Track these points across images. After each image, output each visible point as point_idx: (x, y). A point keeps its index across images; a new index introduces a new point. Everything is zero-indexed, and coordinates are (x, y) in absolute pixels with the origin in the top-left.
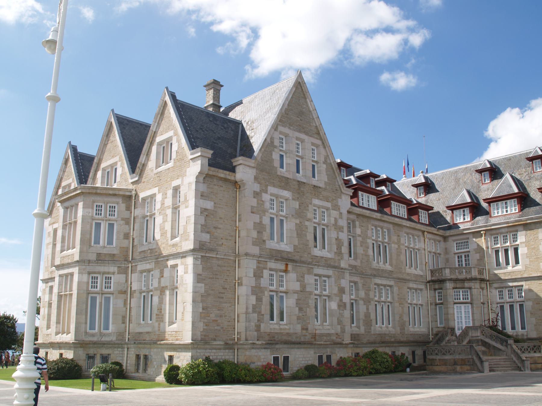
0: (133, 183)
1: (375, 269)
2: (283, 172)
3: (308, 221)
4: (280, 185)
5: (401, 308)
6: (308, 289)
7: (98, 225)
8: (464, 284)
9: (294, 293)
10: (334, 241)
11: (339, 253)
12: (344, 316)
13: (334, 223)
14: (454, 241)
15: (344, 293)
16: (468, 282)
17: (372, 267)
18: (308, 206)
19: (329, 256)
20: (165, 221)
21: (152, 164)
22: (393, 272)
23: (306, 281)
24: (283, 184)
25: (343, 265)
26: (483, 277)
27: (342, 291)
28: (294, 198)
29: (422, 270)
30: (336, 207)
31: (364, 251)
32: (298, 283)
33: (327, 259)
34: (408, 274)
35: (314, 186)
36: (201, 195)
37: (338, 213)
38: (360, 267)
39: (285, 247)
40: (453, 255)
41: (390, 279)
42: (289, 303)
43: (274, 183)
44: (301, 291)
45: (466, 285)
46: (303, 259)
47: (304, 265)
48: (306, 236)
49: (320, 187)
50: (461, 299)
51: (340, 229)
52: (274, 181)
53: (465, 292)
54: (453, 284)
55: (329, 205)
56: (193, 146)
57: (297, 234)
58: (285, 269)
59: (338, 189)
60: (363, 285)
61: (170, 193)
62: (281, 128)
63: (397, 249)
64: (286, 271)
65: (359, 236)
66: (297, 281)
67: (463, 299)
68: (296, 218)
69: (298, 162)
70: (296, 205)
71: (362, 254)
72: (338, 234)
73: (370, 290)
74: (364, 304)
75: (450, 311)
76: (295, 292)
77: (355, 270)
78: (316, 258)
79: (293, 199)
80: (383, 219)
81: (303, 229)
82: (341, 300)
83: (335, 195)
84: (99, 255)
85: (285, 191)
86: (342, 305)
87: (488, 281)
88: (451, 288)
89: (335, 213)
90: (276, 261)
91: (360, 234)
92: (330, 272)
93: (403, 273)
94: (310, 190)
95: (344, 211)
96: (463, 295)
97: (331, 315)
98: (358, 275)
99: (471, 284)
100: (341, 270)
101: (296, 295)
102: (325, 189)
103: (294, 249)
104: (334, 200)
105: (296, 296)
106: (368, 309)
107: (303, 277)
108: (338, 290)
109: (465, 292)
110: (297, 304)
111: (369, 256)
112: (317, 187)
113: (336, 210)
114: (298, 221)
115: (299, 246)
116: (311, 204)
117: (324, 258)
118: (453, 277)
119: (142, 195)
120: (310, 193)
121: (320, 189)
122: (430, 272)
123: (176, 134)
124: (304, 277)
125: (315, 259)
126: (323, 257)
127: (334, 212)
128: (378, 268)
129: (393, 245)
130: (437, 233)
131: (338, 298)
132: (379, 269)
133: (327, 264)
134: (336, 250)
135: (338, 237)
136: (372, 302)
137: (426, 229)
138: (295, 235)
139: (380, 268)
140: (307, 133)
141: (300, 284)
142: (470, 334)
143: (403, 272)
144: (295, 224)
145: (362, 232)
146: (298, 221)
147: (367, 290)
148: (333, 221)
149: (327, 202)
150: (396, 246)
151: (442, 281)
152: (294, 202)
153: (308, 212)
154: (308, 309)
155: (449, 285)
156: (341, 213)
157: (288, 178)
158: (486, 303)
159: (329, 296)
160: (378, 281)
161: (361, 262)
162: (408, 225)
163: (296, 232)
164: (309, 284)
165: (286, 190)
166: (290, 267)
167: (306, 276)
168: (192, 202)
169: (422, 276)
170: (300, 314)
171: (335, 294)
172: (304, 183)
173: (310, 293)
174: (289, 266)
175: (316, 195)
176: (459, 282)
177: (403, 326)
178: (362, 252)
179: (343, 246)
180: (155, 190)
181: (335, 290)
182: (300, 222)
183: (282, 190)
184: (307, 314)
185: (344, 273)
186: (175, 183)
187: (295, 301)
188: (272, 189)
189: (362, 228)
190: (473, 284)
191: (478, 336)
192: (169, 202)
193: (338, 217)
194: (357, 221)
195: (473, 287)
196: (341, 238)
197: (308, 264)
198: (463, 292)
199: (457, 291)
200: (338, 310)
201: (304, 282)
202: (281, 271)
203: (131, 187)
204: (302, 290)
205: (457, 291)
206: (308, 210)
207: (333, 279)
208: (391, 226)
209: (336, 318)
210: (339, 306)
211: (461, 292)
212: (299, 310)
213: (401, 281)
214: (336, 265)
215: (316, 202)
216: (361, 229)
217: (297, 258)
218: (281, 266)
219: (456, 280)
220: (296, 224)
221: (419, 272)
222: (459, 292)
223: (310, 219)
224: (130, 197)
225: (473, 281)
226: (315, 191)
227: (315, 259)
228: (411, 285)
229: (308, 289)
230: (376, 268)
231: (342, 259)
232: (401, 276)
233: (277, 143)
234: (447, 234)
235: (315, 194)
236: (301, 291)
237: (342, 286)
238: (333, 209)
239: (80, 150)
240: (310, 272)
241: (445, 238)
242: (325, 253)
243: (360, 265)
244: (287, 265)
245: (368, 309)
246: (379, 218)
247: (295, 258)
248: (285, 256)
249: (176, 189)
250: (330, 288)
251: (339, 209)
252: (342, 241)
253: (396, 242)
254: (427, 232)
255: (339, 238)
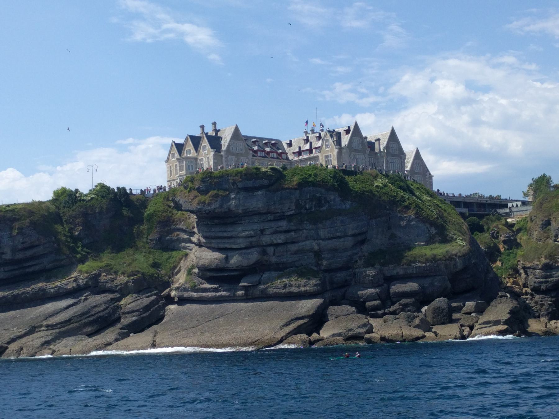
0: (197, 155)
7: (189, 166)
20: (206, 165)
21: (201, 151)
30: (248, 158)
36: (214, 159)
56: (212, 148)
61: (207, 158)
62: (232, 141)
69: (237, 148)
84: (190, 173)
119: (199, 158)
123: (207, 144)
140: (239, 140)
168: (212, 161)
180: (203, 157)
186: (208, 156)
188: (230, 156)
192: (207, 160)
203: (196, 156)
224: (196, 158)
233: (231, 145)
239: (176, 142)
249: (208, 158)
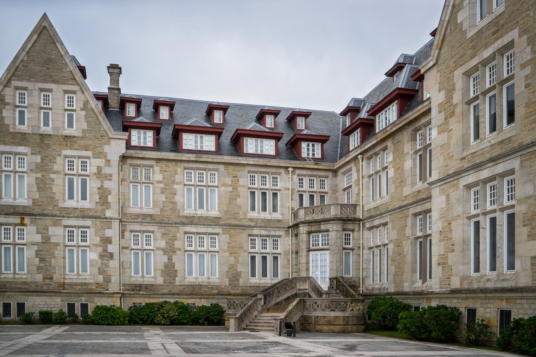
1: (186, 217)
2: (24, 128)
3: (55, 173)
4: (14, 142)
5: (233, 258)
6: (53, 240)
8: (320, 227)
9: (33, 245)
10: (96, 190)
11: (104, 201)
12: (109, 266)
13: (96, 172)
14: (344, 174)
15: (110, 242)
16: (324, 223)
17: (181, 215)
18: (55, 159)
19: (93, 206)
22: (220, 218)
23: (50, 233)
24: (18, 140)
25: (109, 214)
26: (351, 216)
27: (107, 241)
28: (34, 152)
29: (282, 214)
31: (167, 198)
32: (40, 235)
33: (82, 210)
34: (251, 220)
35: (66, 136)
37: (104, 160)
38: (159, 215)
39: (23, 201)
40: (342, 192)
41: (212, 227)
42: (29, 253)
43: (4, 141)
44: (43, 243)
45: (323, 227)
46: (45, 212)
47: (47, 218)
48: (51, 189)
49: (74, 137)
50: (320, 245)
51: (109, 177)
52: (6, 139)
53: (325, 237)
54: (307, 227)
55: (89, 153)
57: (38, 188)
58: (20, 223)
59: (105, 135)
60: (162, 234)
63: (230, 192)
64: (22, 224)
65: (159, 182)
66: (37, 233)
67: (322, 245)
68: (37, 172)
70: (38, 159)
71: (164, 202)
72: (102, 182)
73: (176, 240)
74: (164, 255)
75: (303, 260)
76: (37, 244)
77: (150, 219)
78: (67, 209)
79: (32, 154)
80: (201, 160)
81: (47, 182)
82: (105, 250)
83: (99, 142)
85: (20, 147)
86: (107, 256)
87: (360, 220)
88: (305, 232)
89: (100, 162)
90: (6, 216)
91: (162, 180)
92: (88, 222)
93: (241, 219)
94: (59, 141)
95: (115, 158)
96: (322, 241)
97: (92, 265)
98: (154, 224)
99: (329, 226)
100: (105, 220)
101: (36, 246)
102: (83, 138)
103: (33, 203)
104: (98, 147)
105: (36, 248)
106: (170, 259)
107: (47, 229)
108: (100, 240)
109: (325, 237)
110: (36, 255)
111: (176, 203)
112: (70, 137)
113: (101, 158)
114: (39, 175)
115: (40, 200)
116: (60, 155)
117: (79, 209)
118: (309, 218)
120: (59, 144)
121: (75, 139)
122: (293, 215)
124: (48, 229)
125: (63, 211)
126: (77, 208)
127: (96, 160)
128: (191, 215)
129: (223, 188)
130: (316, 167)
131: (100, 249)
132: (193, 216)
133: (83, 214)
134: (98, 200)
135: (102, 186)
136: (177, 252)
137: (291, 164)
138: (35, 188)
139: (195, 215)
141: (42, 236)
142: (298, 287)
143: (241, 217)
144: (34, 178)
145: (164, 178)
146: (39, 175)
147: (170, 240)
148: (94, 170)
149: (86, 150)
150: (230, 189)
151: (296, 226)
152: (33, 156)
153: (55, 164)
154: (53, 260)
155: (303, 229)
156: (109, 160)
157: (25, 133)
158: (356, 248)
159: (88, 247)
160: (188, 229)
161: (162, 210)
162: (251, 163)
163: (36, 187)
164: (55, 236)
165: (22, 146)
166: (27, 220)
167: (51, 229)
169: (279, 221)
170: (42, 265)
171: (96, 245)
172: (50, 135)
173: (57, 244)
174: (25, 219)
175: (69, 146)
176: (314, 224)
177: (235, 277)
178: (164, 200)
179: (110, 195)
181: (97, 240)
182: (43, 176)
183: (16, 147)
184: (52, 265)
185: (111, 223)
187: (34, 253)
189: (166, 173)
190: (330, 226)
191: (306, 289)
193: (103, 165)
194: (157, 166)
195: (330, 230)
196: (108, 187)
197: (53, 216)
198: (322, 237)
199: (316, 236)
200: (100, 261)
201: (48, 233)
202: (16, 225)
204: (44, 241)
205: (316, 236)
206: (55, 162)
207: (93, 230)
208: (222, 168)
209: (97, 269)
210: (101, 257)
211: (320, 238)
212: (40, 260)
213: (235, 228)
214: (98, 215)
215: (69, 152)
216: (163, 175)
217: (37, 211)
218: (17, 220)
219: (309, 223)
220: (36, 178)
221: (277, 216)
222: (318, 237)
223: (58, 171)
225: (332, 222)
226: (66, 141)
227: (63, 211)
228: (255, 231)
229: (53, 240)
230: (188, 215)
231: (107, 208)
232: (233, 222)
234: (335, 167)
235: (66, 145)
236: (43, 243)
237: (107, 235)
238: (94, 158)
240: (55, 224)
241: (335, 172)
242: (86, 204)
243: (159, 214)
244: (22, 219)
245: (170, 259)
246: (193, 159)
247: (35, 212)
248: (20, 210)
250: (92, 238)
251: (106, 156)
252: (110, 189)
253: (230, 183)
254: (292, 167)
255: (104, 187)
